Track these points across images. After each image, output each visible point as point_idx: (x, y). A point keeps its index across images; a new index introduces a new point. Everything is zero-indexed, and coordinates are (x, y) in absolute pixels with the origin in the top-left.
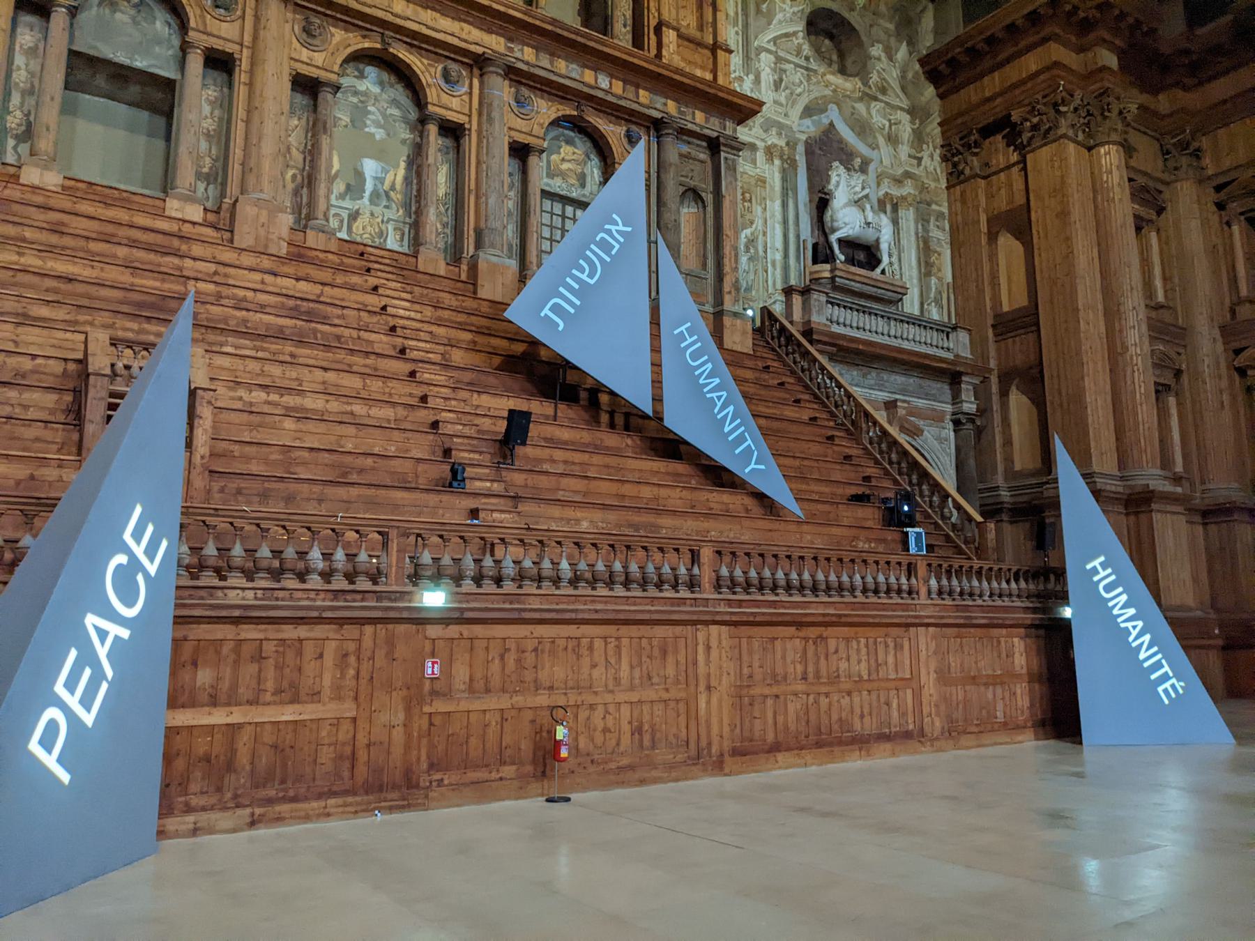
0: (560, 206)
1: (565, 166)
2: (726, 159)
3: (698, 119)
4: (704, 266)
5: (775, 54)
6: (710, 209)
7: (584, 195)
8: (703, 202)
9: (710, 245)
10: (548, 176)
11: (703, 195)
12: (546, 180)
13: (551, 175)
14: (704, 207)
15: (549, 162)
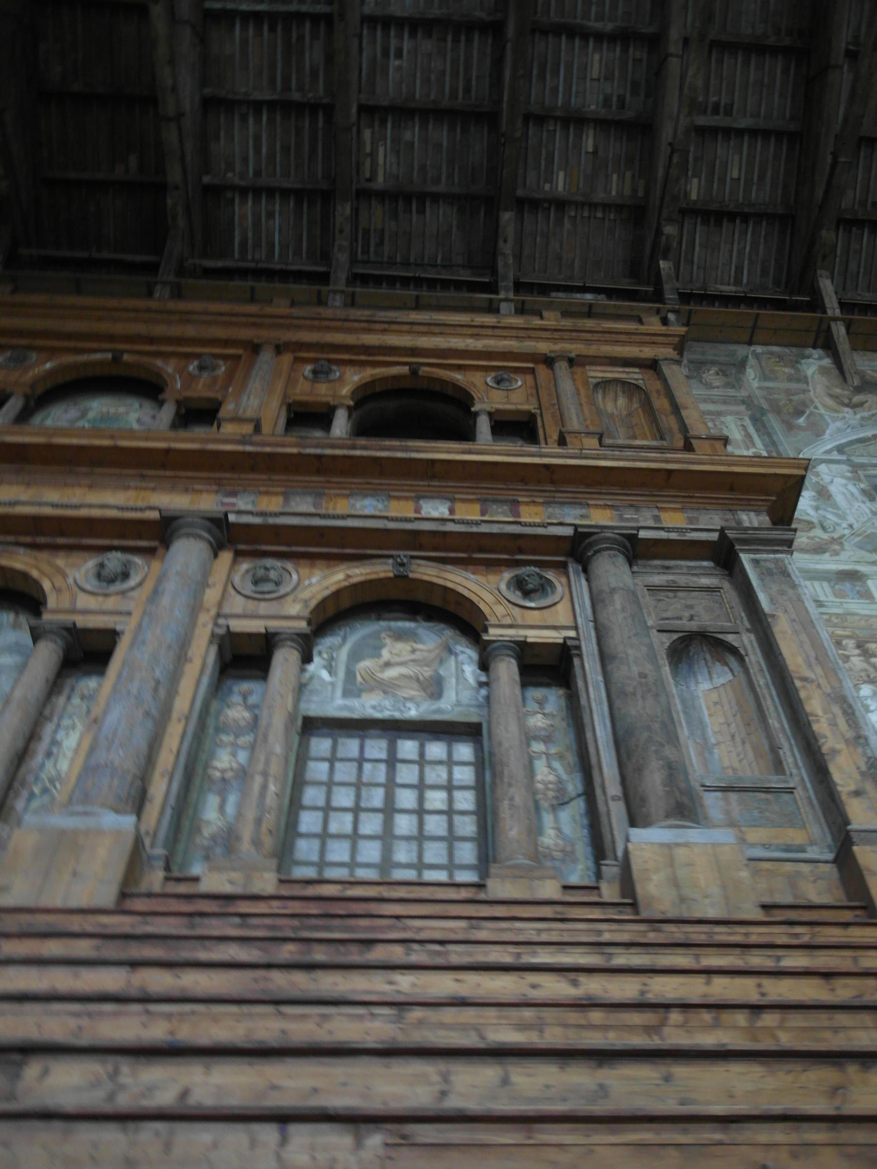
0: (383, 744)
1: (391, 673)
2: (756, 562)
3: (672, 521)
4: (778, 766)
5: (849, 462)
6: (755, 657)
7: (439, 711)
8: (734, 651)
9: (778, 720)
10: (346, 694)
11: (730, 638)
12: (339, 701)
13: (351, 689)
14: (741, 659)
15: (350, 675)
